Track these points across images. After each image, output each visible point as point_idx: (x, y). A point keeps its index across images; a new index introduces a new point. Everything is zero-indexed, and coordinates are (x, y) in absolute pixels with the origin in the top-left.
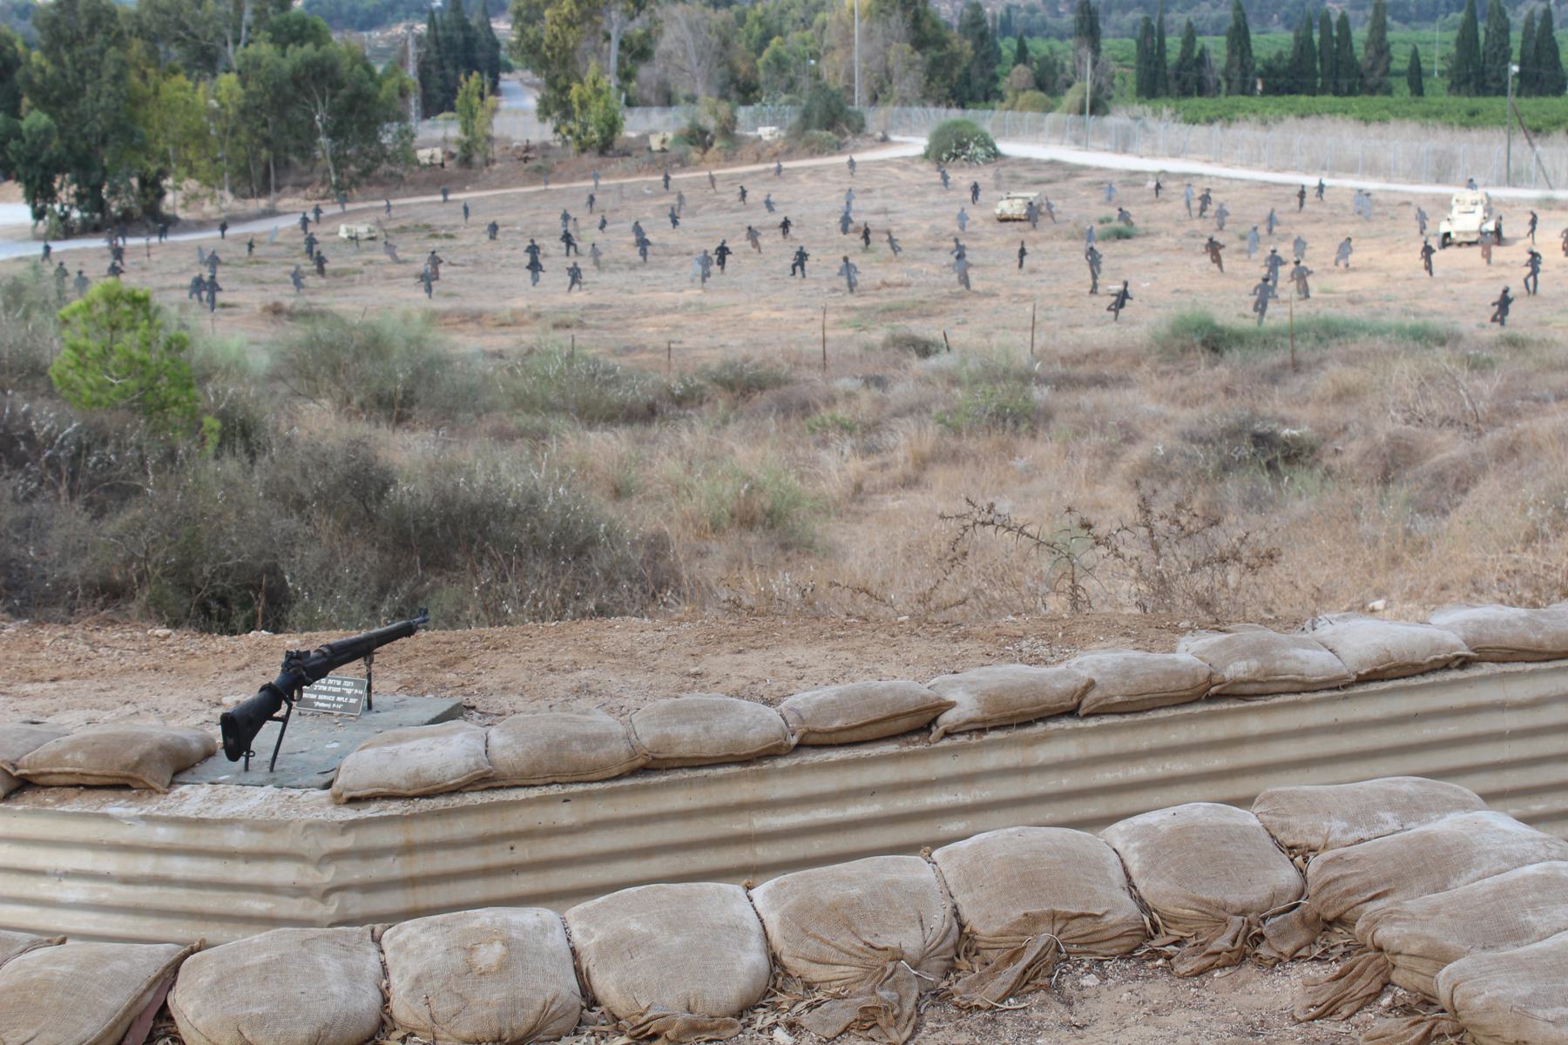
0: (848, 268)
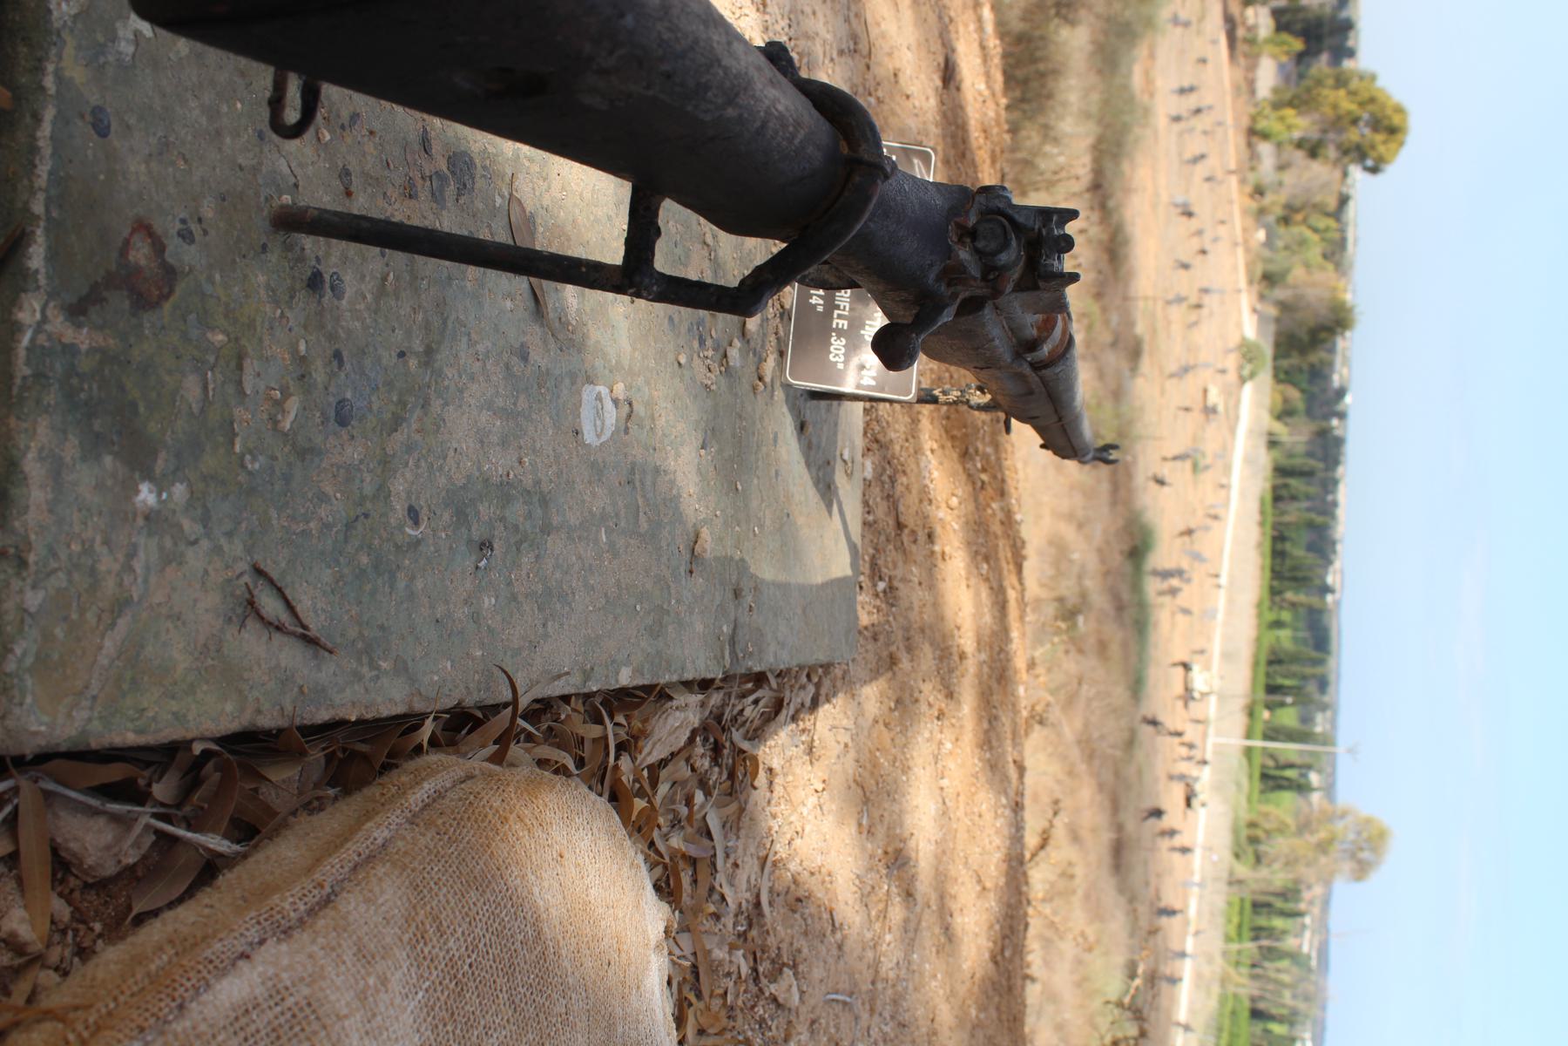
0: (1180, 300)
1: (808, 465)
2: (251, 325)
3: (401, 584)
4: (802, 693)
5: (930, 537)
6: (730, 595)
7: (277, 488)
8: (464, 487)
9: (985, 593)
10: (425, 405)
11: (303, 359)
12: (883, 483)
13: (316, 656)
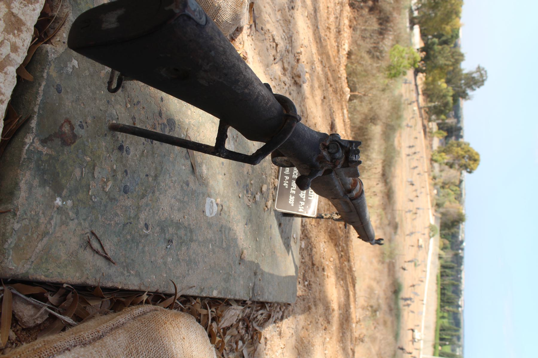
0: (410, 211)
1: (282, 237)
2: (99, 157)
3: (140, 247)
4: (278, 314)
5: (323, 269)
6: (253, 274)
7: (102, 208)
8: (164, 221)
9: (341, 291)
10: (154, 192)
11: (115, 171)
12: (308, 250)
13: (109, 264)
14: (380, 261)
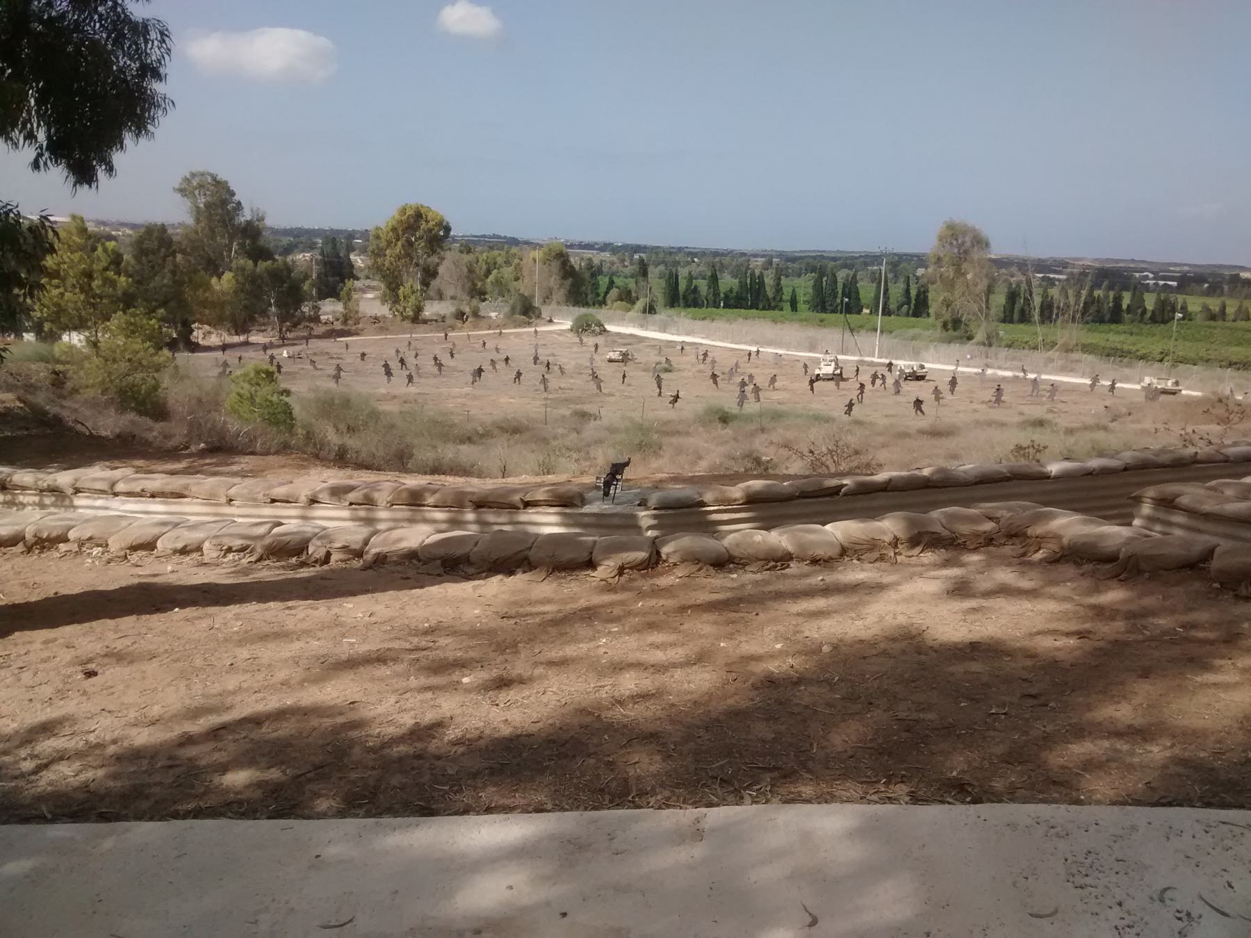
0: (544, 380)
14: (656, 455)
